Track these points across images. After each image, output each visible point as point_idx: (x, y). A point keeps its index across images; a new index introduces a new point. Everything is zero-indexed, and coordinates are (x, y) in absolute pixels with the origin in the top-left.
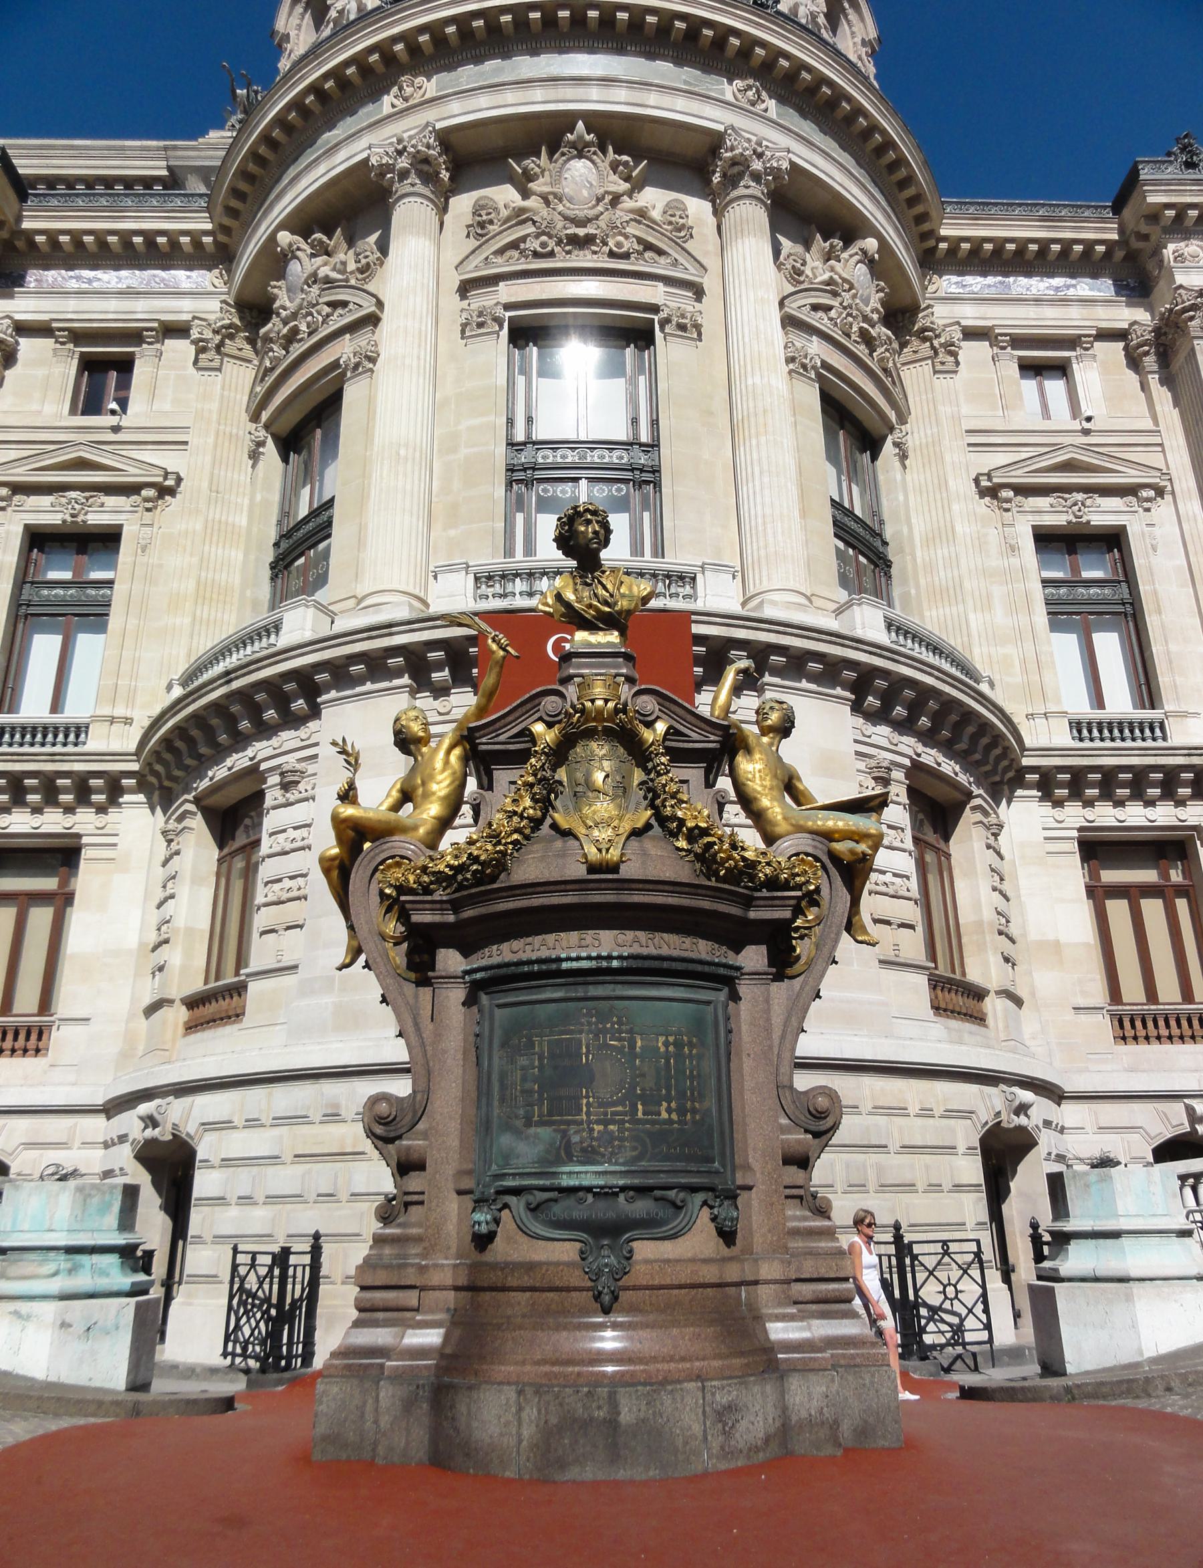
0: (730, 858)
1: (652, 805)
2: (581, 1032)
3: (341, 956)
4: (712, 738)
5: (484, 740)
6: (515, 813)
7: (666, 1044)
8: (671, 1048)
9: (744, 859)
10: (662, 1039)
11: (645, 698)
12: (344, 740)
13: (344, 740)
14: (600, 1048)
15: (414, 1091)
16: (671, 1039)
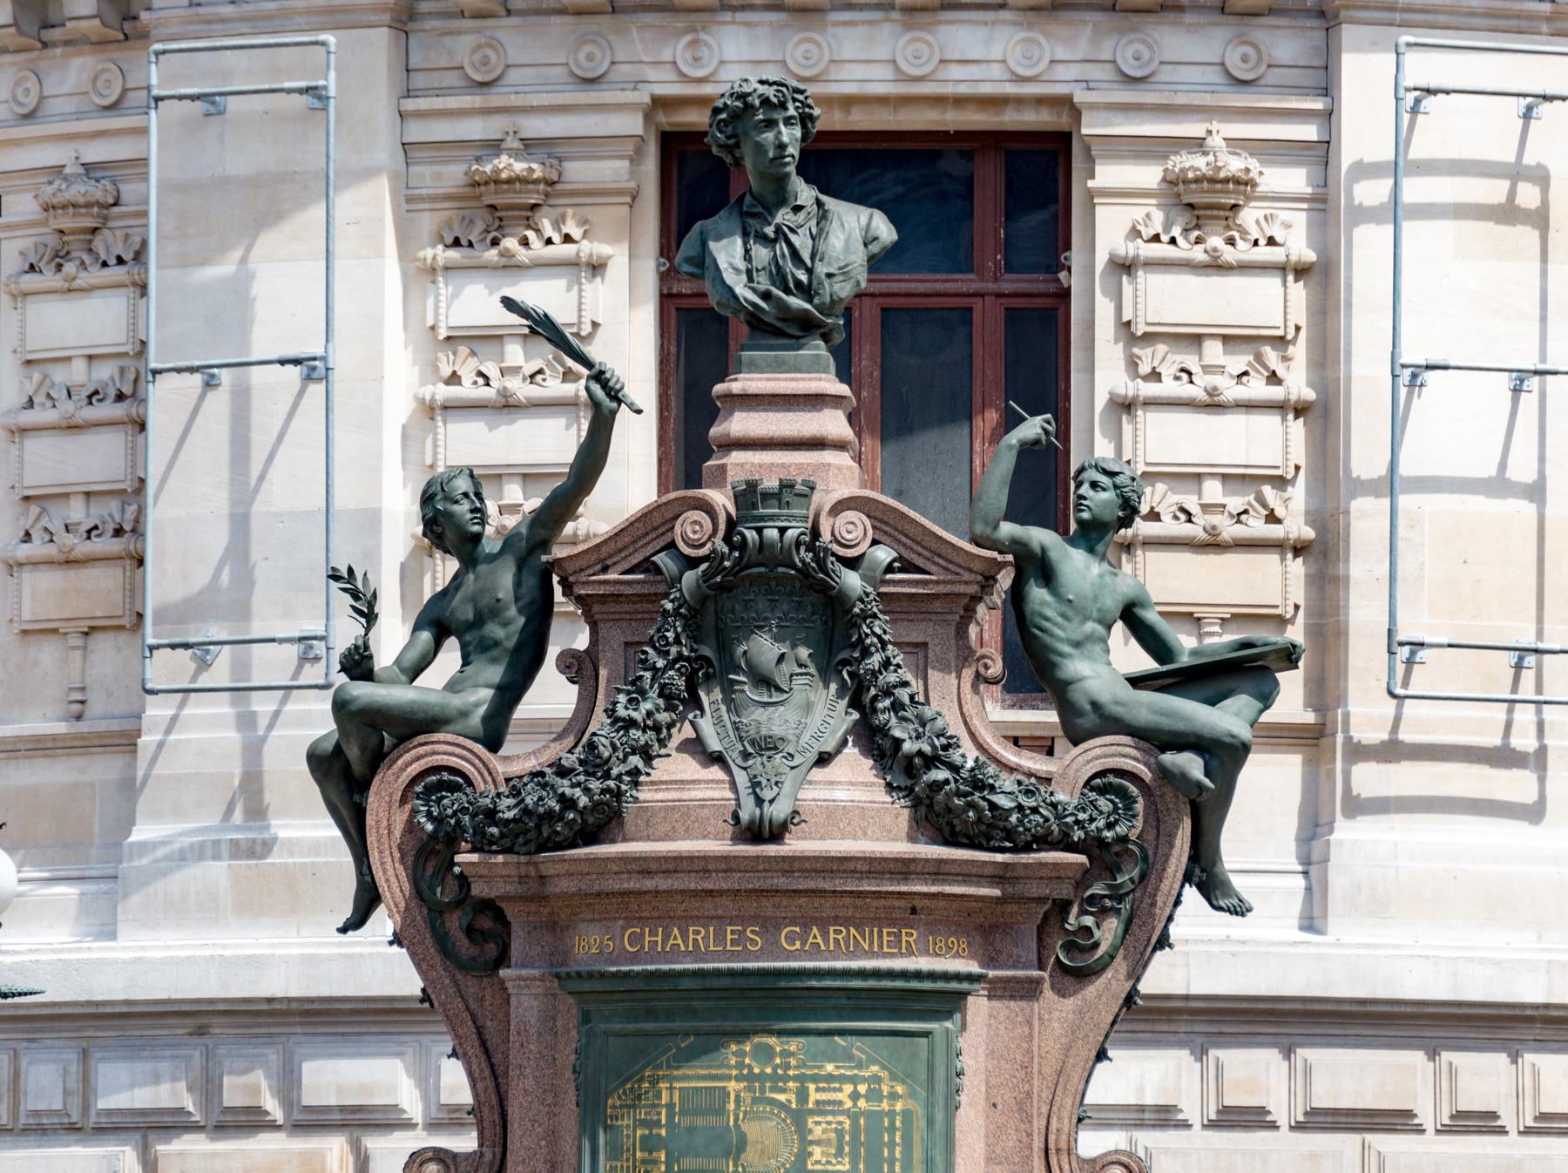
0: (972, 805)
1: (855, 704)
2: (729, 1078)
3: (347, 911)
4: (966, 576)
5: (582, 577)
6: (631, 723)
7: (855, 1096)
8: (862, 1103)
9: (993, 806)
10: (848, 1088)
11: (851, 515)
12: (350, 571)
13: (350, 571)
14: (755, 1101)
15: (481, 1145)
16: (862, 1089)
